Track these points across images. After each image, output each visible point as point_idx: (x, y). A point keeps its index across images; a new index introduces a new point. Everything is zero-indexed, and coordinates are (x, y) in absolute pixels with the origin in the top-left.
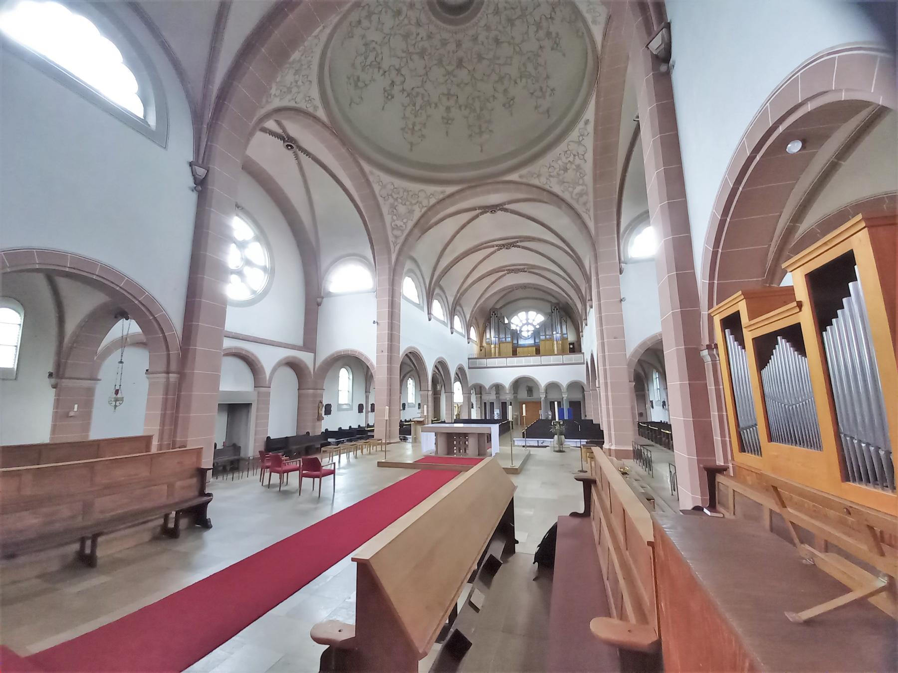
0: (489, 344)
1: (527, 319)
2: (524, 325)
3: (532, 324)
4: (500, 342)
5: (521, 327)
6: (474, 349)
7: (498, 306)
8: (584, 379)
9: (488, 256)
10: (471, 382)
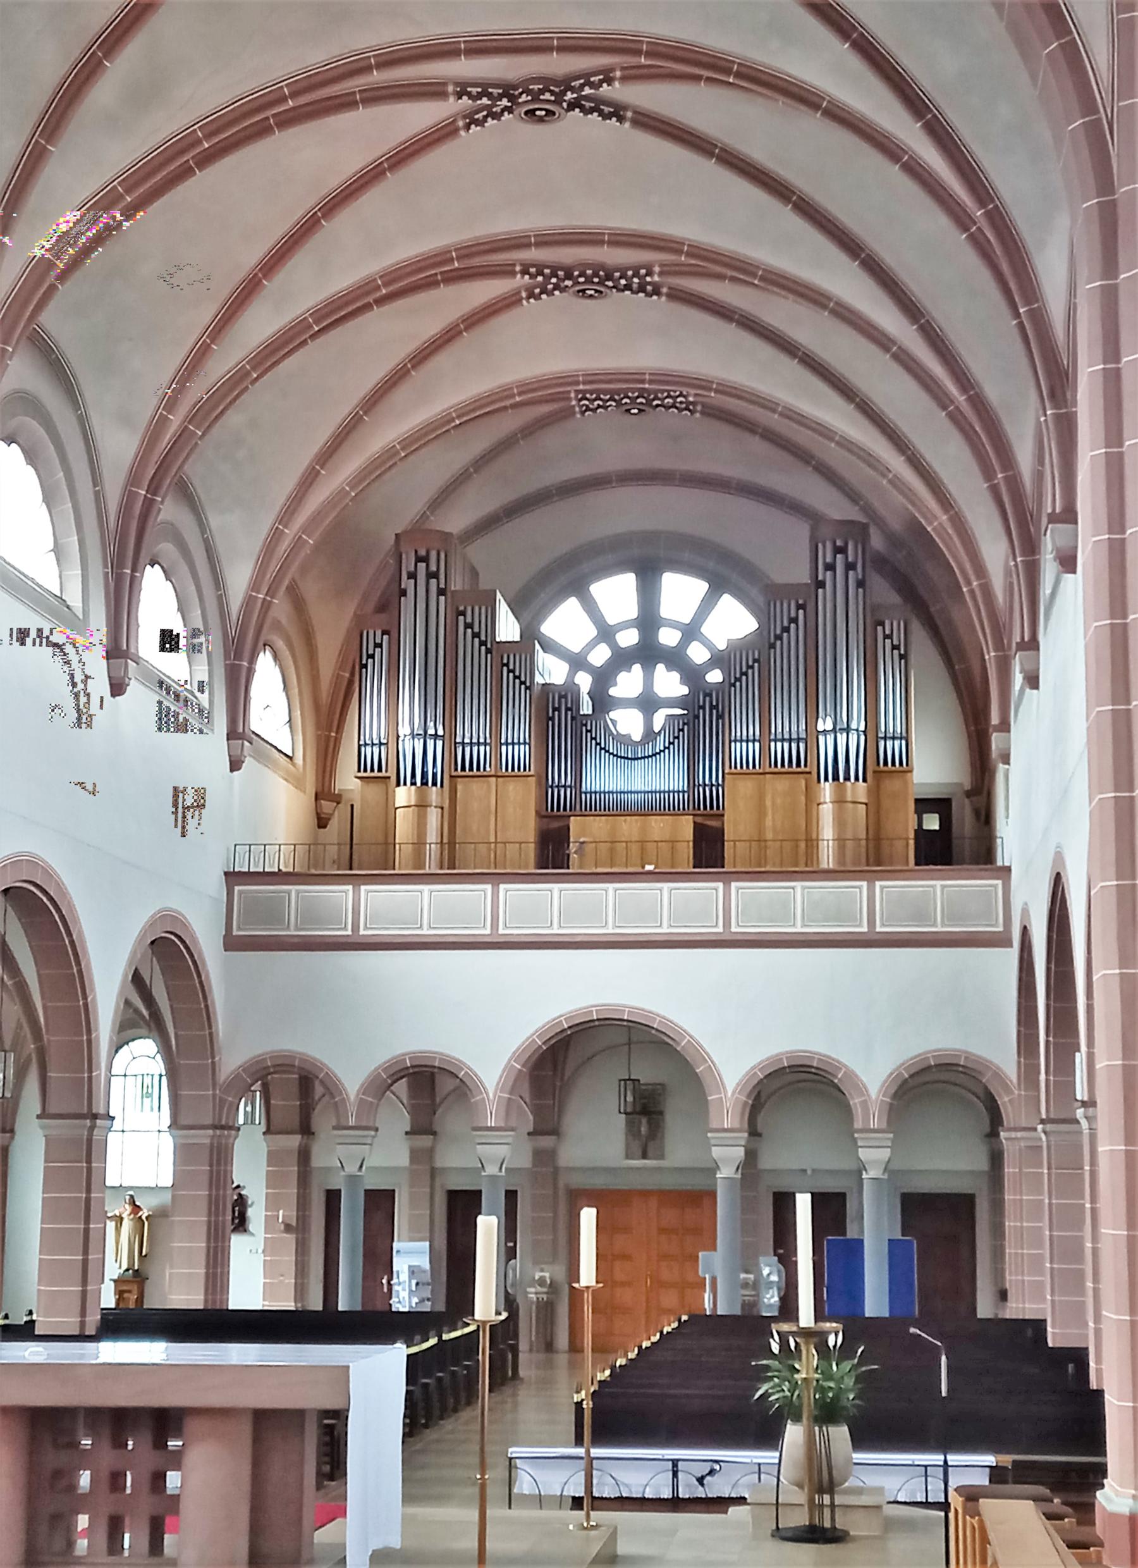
0: (377, 776)
1: (648, 621)
2: (622, 659)
3: (675, 659)
4: (461, 770)
5: (603, 677)
6: (271, 811)
7: (455, 521)
8: (992, 1041)
9: (402, 156)
10: (238, 1046)
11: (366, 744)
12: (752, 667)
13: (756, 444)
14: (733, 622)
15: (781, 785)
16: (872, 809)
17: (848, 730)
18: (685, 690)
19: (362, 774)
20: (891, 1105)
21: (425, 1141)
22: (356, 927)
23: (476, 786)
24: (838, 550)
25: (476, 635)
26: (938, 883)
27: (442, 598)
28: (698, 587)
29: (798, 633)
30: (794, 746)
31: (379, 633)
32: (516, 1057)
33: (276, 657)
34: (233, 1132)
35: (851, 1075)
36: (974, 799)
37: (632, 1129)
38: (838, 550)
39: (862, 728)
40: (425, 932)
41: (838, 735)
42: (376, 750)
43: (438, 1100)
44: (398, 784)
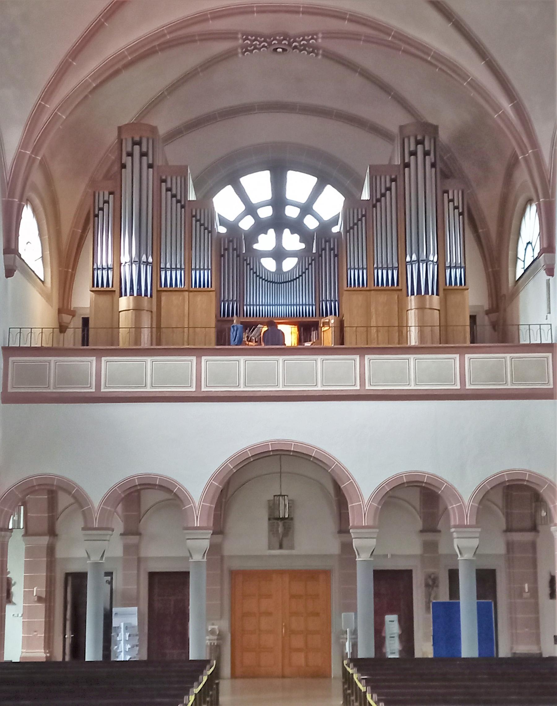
0: (106, 291)
1: (279, 201)
2: (261, 227)
3: (296, 226)
11: (98, 269)
12: (360, 220)
13: (355, 81)
14: (331, 204)
15: (382, 298)
16: (443, 312)
17: (427, 261)
18: (303, 246)
19: (95, 288)
20: (478, 508)
21: (133, 540)
22: (98, 386)
23: (175, 299)
24: (418, 143)
25: (174, 196)
26: (508, 356)
27: (151, 170)
28: (311, 181)
29: (390, 199)
30: (390, 272)
31: (106, 193)
32: (215, 477)
33: (34, 211)
34: (8, 533)
35: (450, 489)
36: (491, 315)
37: (272, 530)
38: (418, 143)
39: (435, 260)
40: (149, 389)
41: (421, 264)
42: (105, 272)
43: (143, 511)
44: (121, 296)
